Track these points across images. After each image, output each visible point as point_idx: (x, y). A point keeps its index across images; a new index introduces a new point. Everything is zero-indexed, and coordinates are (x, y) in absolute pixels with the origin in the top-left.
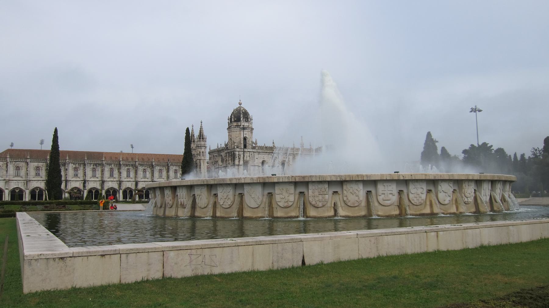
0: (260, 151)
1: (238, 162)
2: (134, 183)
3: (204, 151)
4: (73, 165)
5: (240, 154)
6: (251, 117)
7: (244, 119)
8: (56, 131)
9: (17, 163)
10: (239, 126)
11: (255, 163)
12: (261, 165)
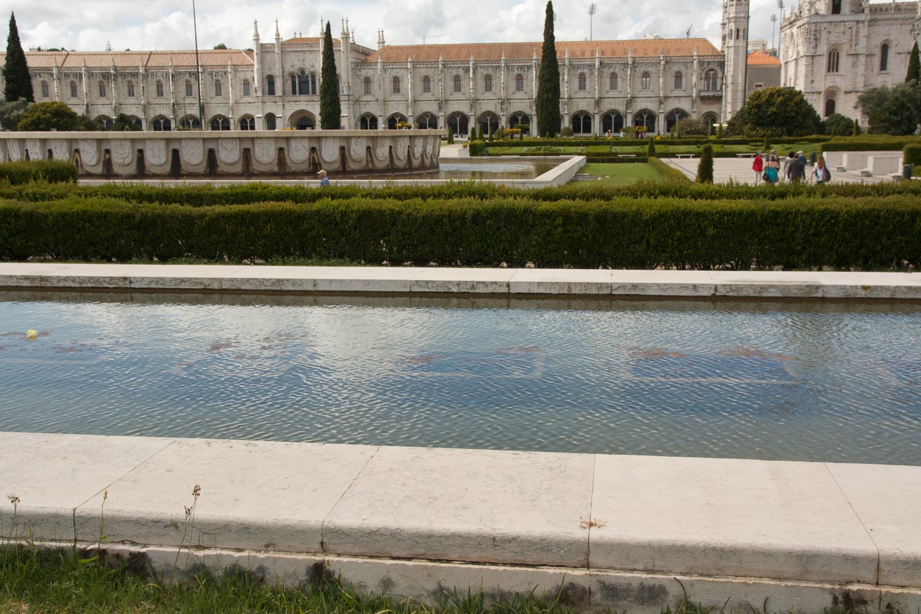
0: (878, 17)
1: (813, 48)
4: (482, 70)
5: (818, 29)
9: (395, 70)
11: (857, 47)
12: (878, 52)
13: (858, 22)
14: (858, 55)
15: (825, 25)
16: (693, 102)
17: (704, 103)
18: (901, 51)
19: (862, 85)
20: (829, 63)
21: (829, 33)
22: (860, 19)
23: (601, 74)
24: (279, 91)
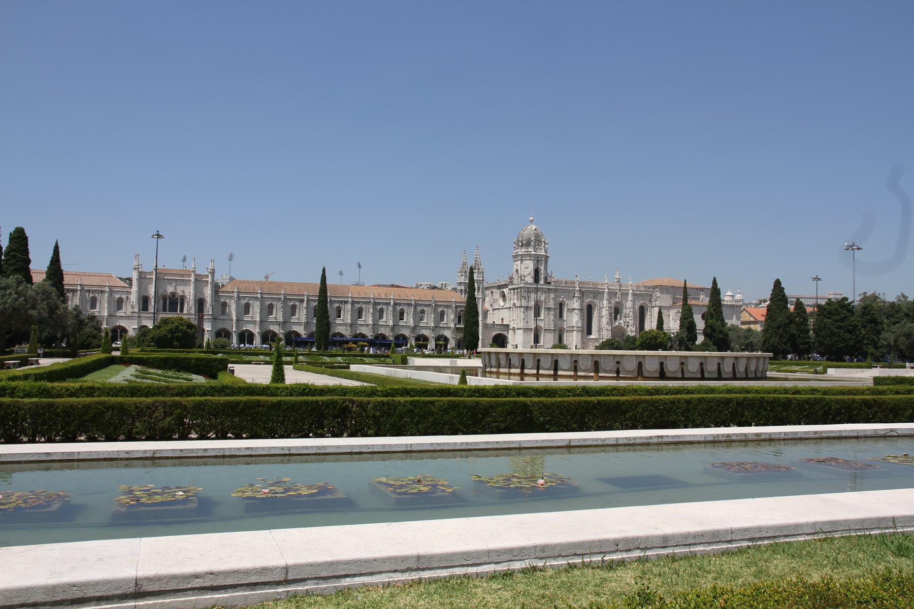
8: (324, 270)
10: (529, 252)
11: (549, 303)
17: (458, 332)
19: (553, 326)
23: (394, 309)
24: (151, 309)
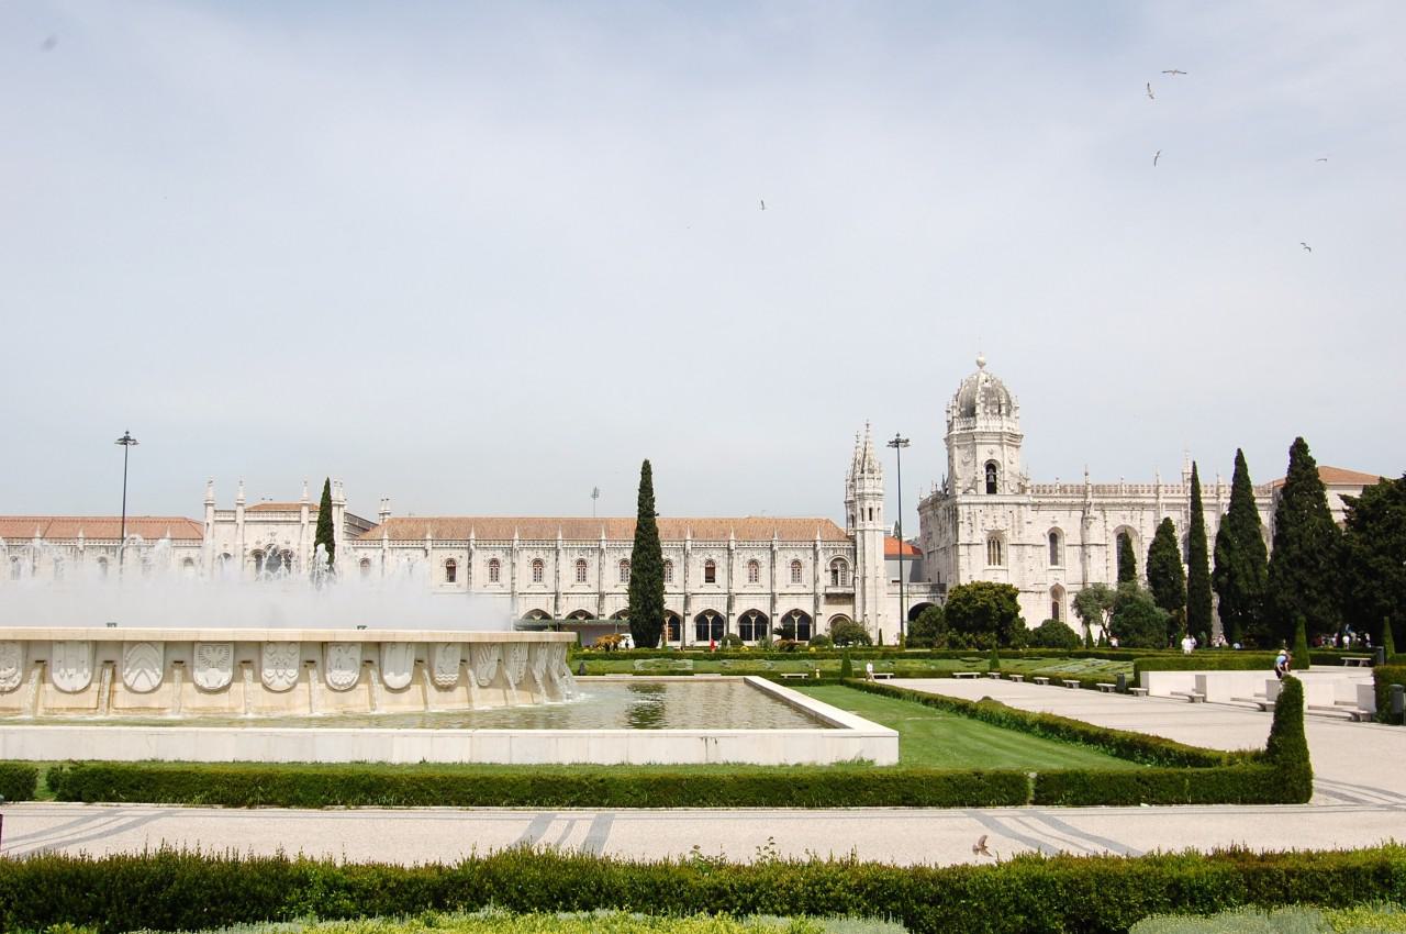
2: (682, 598)
3: (872, 506)
4: (530, 552)
5: (973, 511)
6: (1013, 401)
7: (985, 407)
12: (1047, 542)
13: (1019, 504)
14: (1023, 545)
15: (981, 507)
16: (816, 600)
17: (830, 604)
18: (1073, 543)
20: (989, 555)
21: (987, 516)
22: (1021, 502)
